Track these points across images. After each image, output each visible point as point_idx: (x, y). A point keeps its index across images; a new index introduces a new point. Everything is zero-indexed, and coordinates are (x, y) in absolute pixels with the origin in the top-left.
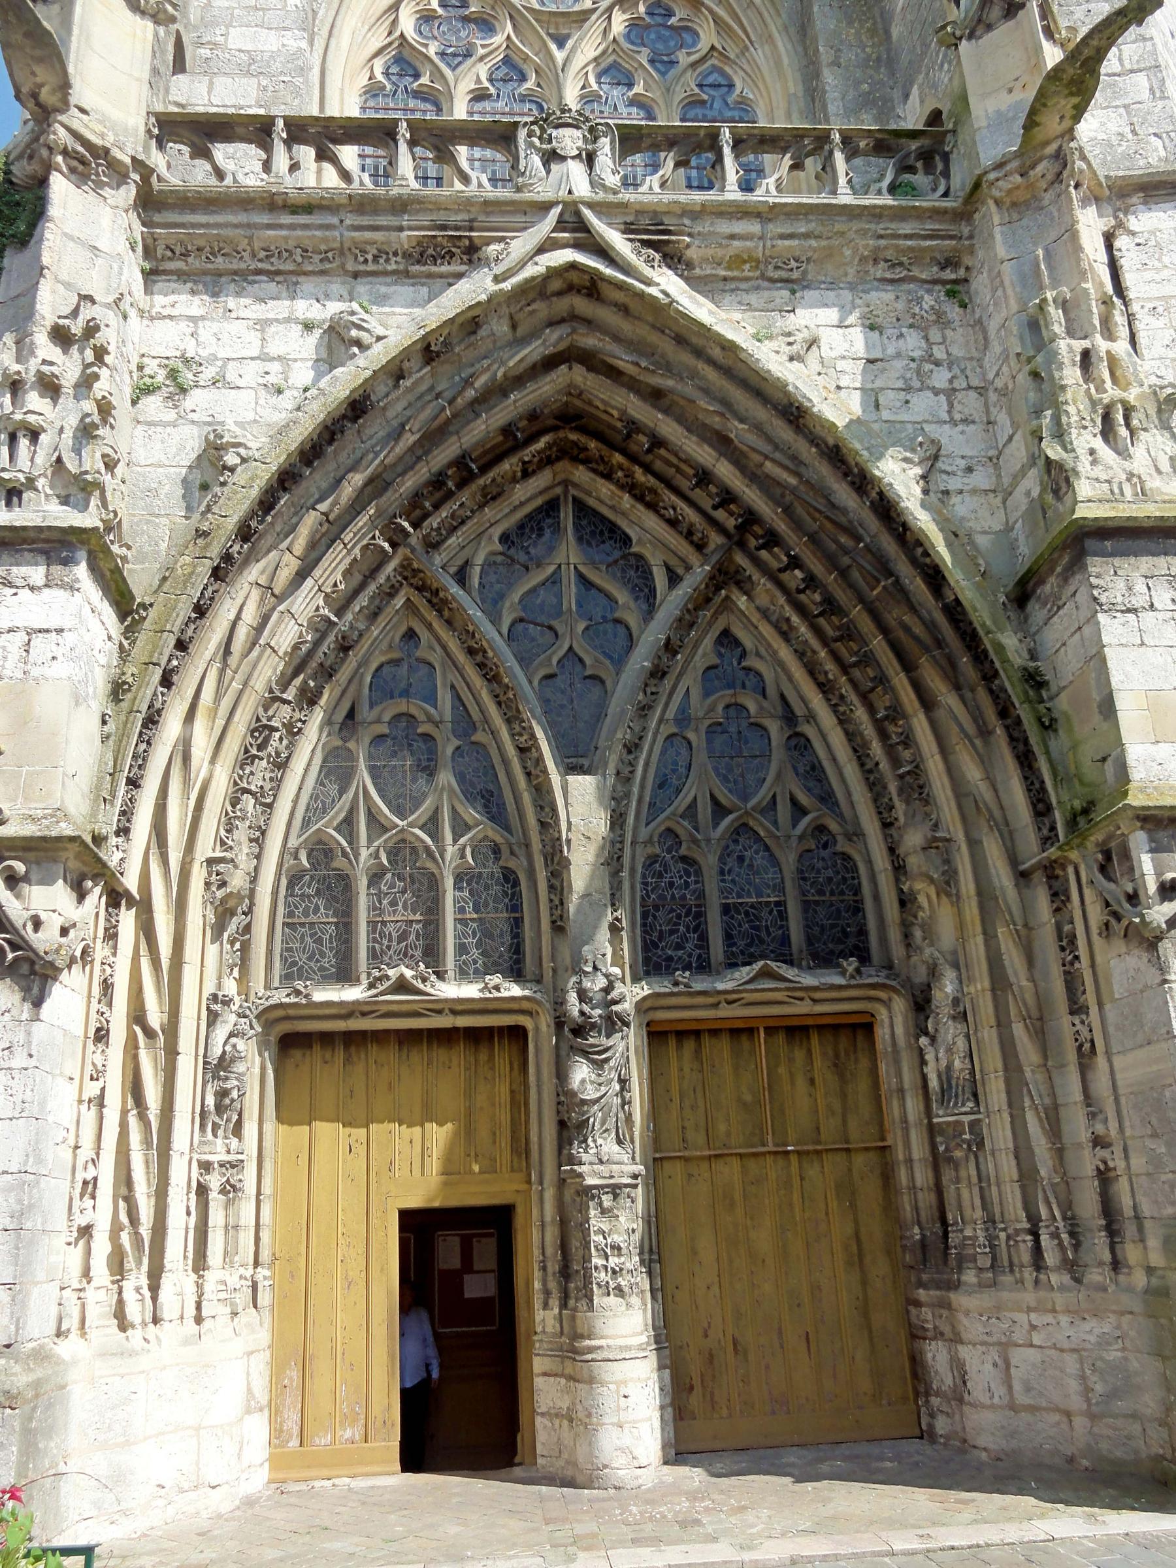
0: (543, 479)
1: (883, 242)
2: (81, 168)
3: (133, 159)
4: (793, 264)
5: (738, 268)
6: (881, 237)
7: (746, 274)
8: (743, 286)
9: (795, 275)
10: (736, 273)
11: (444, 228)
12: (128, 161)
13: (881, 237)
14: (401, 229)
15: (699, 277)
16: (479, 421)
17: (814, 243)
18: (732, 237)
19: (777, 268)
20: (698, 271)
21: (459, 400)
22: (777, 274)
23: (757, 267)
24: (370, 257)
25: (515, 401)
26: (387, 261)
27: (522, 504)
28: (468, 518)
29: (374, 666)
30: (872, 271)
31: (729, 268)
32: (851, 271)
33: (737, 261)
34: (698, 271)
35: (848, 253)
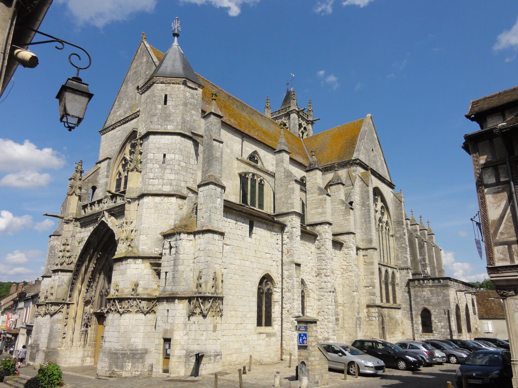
33: (118, 213)
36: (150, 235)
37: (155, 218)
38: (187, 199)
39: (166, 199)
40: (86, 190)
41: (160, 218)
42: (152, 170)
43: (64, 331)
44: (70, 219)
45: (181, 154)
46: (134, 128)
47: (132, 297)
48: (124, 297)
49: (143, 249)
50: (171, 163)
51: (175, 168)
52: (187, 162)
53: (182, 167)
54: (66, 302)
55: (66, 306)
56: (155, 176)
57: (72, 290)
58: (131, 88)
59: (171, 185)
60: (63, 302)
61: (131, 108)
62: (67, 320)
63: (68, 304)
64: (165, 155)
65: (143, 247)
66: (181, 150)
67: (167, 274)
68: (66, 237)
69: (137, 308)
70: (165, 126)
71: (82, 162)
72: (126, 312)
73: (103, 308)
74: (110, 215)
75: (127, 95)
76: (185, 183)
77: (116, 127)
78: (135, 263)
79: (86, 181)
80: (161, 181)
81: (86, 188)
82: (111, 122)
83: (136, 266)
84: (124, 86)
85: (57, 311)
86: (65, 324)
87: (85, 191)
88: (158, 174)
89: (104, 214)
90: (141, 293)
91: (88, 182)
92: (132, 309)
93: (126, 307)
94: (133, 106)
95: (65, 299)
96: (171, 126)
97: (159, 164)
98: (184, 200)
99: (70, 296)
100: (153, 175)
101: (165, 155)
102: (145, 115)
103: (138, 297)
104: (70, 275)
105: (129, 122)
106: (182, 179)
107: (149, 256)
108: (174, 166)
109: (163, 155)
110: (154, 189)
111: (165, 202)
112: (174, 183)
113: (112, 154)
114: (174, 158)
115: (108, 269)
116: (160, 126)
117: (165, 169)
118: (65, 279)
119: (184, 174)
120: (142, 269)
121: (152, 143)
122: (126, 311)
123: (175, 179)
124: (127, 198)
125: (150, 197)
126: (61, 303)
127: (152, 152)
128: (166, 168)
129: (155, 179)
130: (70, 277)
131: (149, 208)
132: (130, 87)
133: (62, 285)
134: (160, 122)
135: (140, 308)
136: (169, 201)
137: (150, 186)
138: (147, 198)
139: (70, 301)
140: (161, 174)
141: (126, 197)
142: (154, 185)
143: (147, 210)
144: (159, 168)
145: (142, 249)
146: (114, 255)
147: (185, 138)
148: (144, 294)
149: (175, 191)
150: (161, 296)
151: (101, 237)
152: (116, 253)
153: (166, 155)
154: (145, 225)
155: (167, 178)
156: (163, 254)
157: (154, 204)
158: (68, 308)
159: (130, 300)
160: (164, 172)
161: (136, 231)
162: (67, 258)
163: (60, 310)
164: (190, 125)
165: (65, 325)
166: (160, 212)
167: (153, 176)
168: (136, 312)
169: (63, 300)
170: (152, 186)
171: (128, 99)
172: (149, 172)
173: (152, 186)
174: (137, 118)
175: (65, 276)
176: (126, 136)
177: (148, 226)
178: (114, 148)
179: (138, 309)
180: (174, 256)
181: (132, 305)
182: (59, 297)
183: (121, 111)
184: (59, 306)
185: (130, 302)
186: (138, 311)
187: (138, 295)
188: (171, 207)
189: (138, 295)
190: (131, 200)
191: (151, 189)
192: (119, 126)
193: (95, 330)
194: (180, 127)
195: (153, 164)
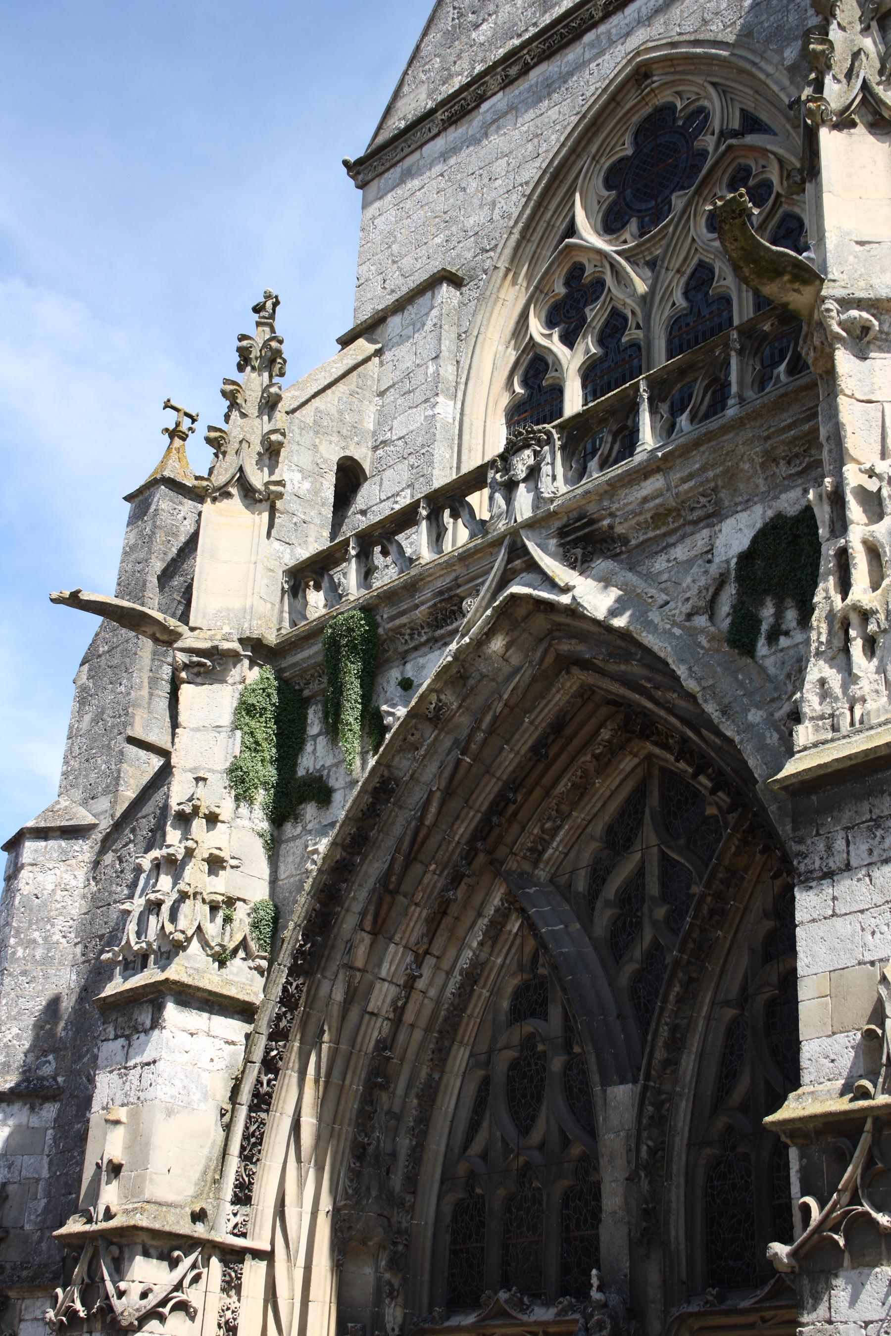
0: (627, 764)
1: (768, 445)
2: (202, 670)
3: (241, 641)
4: (703, 500)
5: (664, 524)
6: (767, 438)
7: (671, 526)
8: (671, 540)
9: (710, 509)
10: (663, 530)
11: (441, 593)
12: (236, 646)
13: (767, 438)
14: (417, 607)
15: (637, 546)
16: (504, 754)
17: (711, 474)
18: (645, 500)
19: (692, 509)
20: (633, 542)
21: (473, 746)
22: (698, 513)
23: (679, 515)
24: (407, 637)
25: (531, 723)
26: (419, 634)
27: (613, 793)
28: (560, 827)
29: (509, 990)
30: (777, 471)
31: (657, 527)
32: (760, 481)
33: (659, 518)
34: (633, 542)
35: (747, 466)
40: (305, 476)
44: (226, 645)
46: (638, 54)
60: (200, 1230)
74: (579, 551)
77: (482, 99)
81: (305, 459)
85: (163, 1303)
113: (469, 255)
115: (505, 1004)
124: (846, 303)
126: (189, 1244)
133: (188, 1106)
139: (244, 1235)
141: (840, 293)
151: (480, 736)
152: (803, 734)
158: (232, 1285)
162: (214, 908)
163: (179, 1296)
169: (199, 1216)
182: (170, 1197)
184: (174, 1264)
192: (507, 83)
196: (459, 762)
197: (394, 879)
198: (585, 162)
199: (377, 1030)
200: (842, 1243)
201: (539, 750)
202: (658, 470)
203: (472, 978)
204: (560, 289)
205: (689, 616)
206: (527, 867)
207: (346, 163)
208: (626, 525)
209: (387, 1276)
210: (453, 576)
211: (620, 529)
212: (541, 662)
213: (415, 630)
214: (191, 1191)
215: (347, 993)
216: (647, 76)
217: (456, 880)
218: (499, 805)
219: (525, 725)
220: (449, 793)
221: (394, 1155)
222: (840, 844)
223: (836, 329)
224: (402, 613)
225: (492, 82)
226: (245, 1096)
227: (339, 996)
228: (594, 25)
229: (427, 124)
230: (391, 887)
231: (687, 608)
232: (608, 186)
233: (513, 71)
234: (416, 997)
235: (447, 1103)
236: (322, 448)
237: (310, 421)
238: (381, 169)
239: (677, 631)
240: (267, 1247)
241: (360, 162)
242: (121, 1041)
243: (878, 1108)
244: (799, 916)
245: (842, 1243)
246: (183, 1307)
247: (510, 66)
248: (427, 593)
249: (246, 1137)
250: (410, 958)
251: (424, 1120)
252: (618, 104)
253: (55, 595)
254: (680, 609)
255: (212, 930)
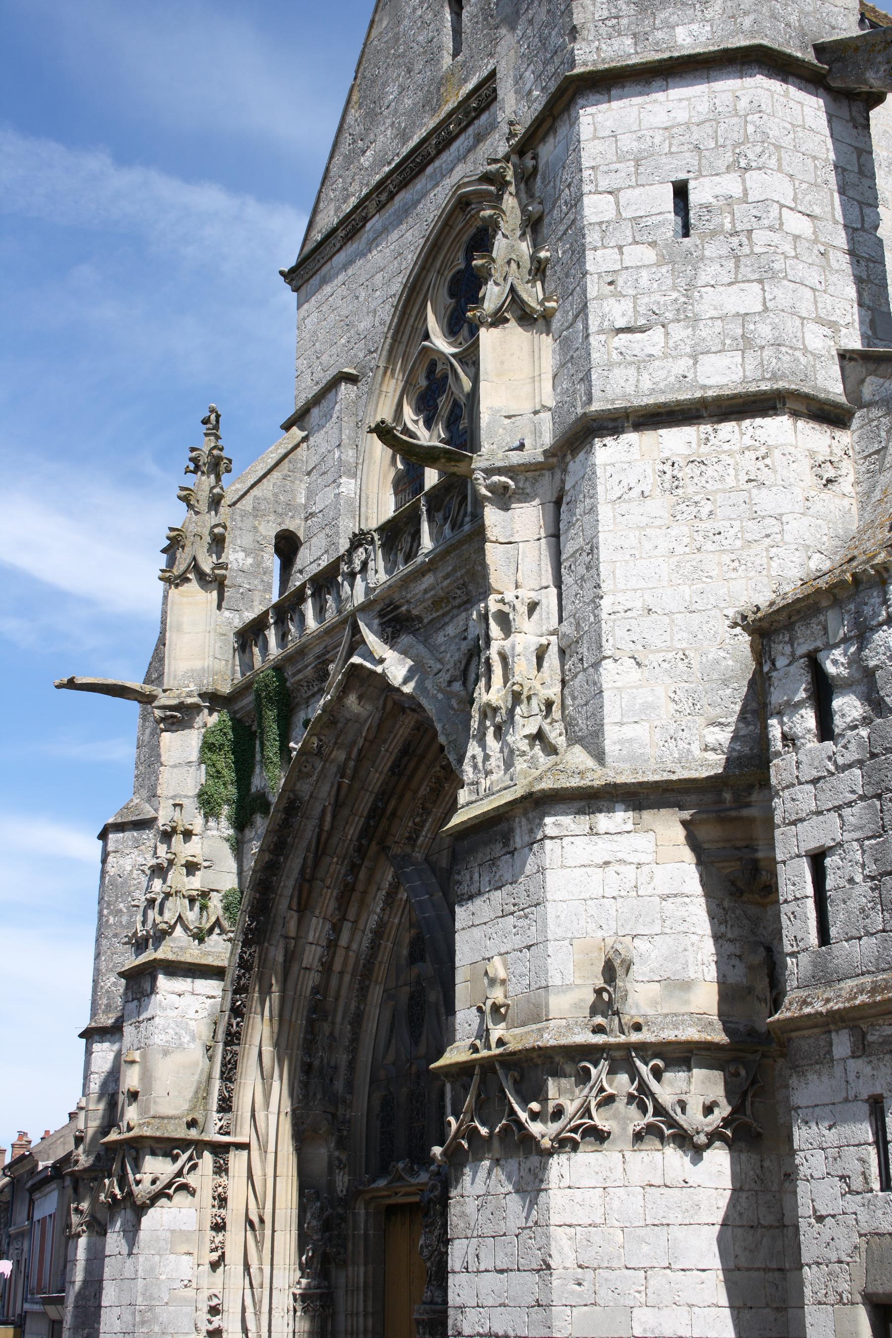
3: (200, 696)
4: (459, 592)
8: (447, 619)
11: (318, 657)
12: (196, 700)
14: (307, 666)
17: (459, 574)
18: (426, 591)
20: (426, 621)
21: (348, 771)
25: (387, 751)
28: (425, 821)
29: (407, 941)
31: (437, 610)
33: (437, 603)
34: (426, 621)
36: (660, 657)
37: (680, 550)
38: (856, 423)
39: (727, 428)
40: (247, 552)
41: (709, 546)
42: (620, 282)
43: (210, 1298)
44: (189, 701)
45: (780, 165)
46: (459, 187)
47: (599, 1039)
48: (552, 1043)
49: (630, 741)
50: (728, 226)
51: (757, 250)
52: (817, 211)
53: (796, 237)
54: (206, 1138)
55: (208, 1158)
56: (642, 310)
57: (229, 1071)
58: (419, 12)
59: (746, 343)
60: (193, 1134)
61: (429, 104)
62: (220, 1237)
63: (220, 1150)
64: (681, 191)
65: (629, 732)
66: (778, 147)
67: (828, 861)
68: (173, 797)
69: (644, 1111)
70: (659, 35)
71: (218, 417)
72: (577, 1137)
73: (401, 1165)
74: (389, 630)
75: (403, 55)
76: (828, 332)
77: (366, 220)
78: (592, 832)
79: (247, 503)
80: (679, 332)
81: (247, 540)
82: (338, 208)
83: (601, 849)
84: (381, 20)
85: (169, 1185)
86: (215, 1256)
87: (247, 555)
88: (656, 297)
89: (356, 630)
90: (651, 1012)
91: (256, 513)
92: (615, 1117)
93: (571, 1107)
94: (441, 84)
95: (201, 1120)
96: (695, 27)
97: (653, 244)
98: (838, 433)
99: (225, 1105)
100: (626, 305)
101: (681, 191)
102: (531, 22)
103: (635, 1037)
104: (212, 987)
105: (429, 170)
106: (805, 308)
107: (674, 777)
108: (749, 238)
109: (668, 191)
110: (646, 384)
111: (726, 447)
112: (764, 331)
113: (361, 355)
114: (737, 192)
115: (405, 952)
116: (629, 41)
117: (695, 261)
118: (191, 1014)
119: (814, 277)
120: (639, 865)
121: (595, 138)
122: (574, 1130)
123: (766, 309)
124: (490, 472)
125: (631, 437)
126: (184, 1144)
127: (604, 184)
128: (702, 258)
129: (642, 330)
130: (212, 1006)
131: (635, 493)
132: (415, 9)
133: (180, 1047)
134: (624, 21)
135: (659, 1110)
136: (749, 442)
137: (616, 371)
138: (608, 440)
139: (228, 1133)
140: (675, 295)
141: (484, 464)
142: (641, 363)
143: (623, 507)
144: (658, 265)
145: (621, 742)
146: (453, 807)
147: (785, 81)
148: (675, 1019)
149: (774, 377)
150: (807, 1010)
151: (352, 764)
152: (463, 796)
153: (691, 185)
154: (621, 597)
155: (715, 314)
156: (777, 745)
157: (661, 467)
158: (221, 1169)
159: (596, 1067)
160: (691, 286)
161: (562, 652)
162: (192, 900)
163: (181, 1180)
164: (801, 11)
165: (214, 1266)
166: (707, 508)
167: (630, 312)
168: (638, 1137)
169: (192, 1124)
170: (632, 371)
171: (409, 71)
172: (600, 298)
173: (632, 371)
174: (470, 130)
175: (188, 999)
176: (422, 241)
177: (638, 604)
178: (363, 325)
179: (650, 1118)
180: (864, 732)
181: (610, 1090)
182: (171, 1112)
183: (381, 138)
184: (175, 1159)
185: (594, 1072)
186: (651, 1129)
187: (638, 1027)
188: (764, 475)
189: (638, 1027)
190: (511, 483)
191: (630, 390)
192: (381, 207)
193: (370, 1294)
194: (747, 22)
195: (620, 248)
196: (340, 785)
197: (308, 871)
198: (432, 276)
199: (312, 979)
200: (466, 1146)
201: (396, 769)
202: (429, 570)
203: (379, 933)
204: (423, 383)
205: (450, 683)
206: (408, 850)
207: (282, 273)
208: (418, 609)
209: (337, 1153)
210: (322, 646)
211: (415, 612)
212: (384, 708)
213: (309, 684)
214: (186, 1106)
215: (285, 956)
216: (468, 204)
217: (354, 869)
218: (376, 813)
219: (383, 753)
220: (338, 805)
221: (336, 1068)
222: (476, 876)
223: (484, 491)
224: (300, 671)
225: (372, 205)
226: (221, 1036)
227: (280, 959)
228: (432, 161)
229: (332, 240)
230: (307, 876)
231: (447, 677)
232: (452, 295)
233: (383, 197)
234: (340, 954)
235: (370, 1026)
236: (261, 528)
237: (249, 508)
238: (307, 276)
239: (440, 696)
240: (246, 1140)
241: (293, 270)
242: (135, 1003)
243: (483, 1058)
244: (458, 925)
245: (466, 1146)
246: (184, 1187)
247: (380, 193)
248: (310, 658)
249: (224, 1065)
250: (328, 926)
251: (355, 1039)
252: (451, 227)
253: (57, 682)
254: (444, 677)
255: (191, 916)
